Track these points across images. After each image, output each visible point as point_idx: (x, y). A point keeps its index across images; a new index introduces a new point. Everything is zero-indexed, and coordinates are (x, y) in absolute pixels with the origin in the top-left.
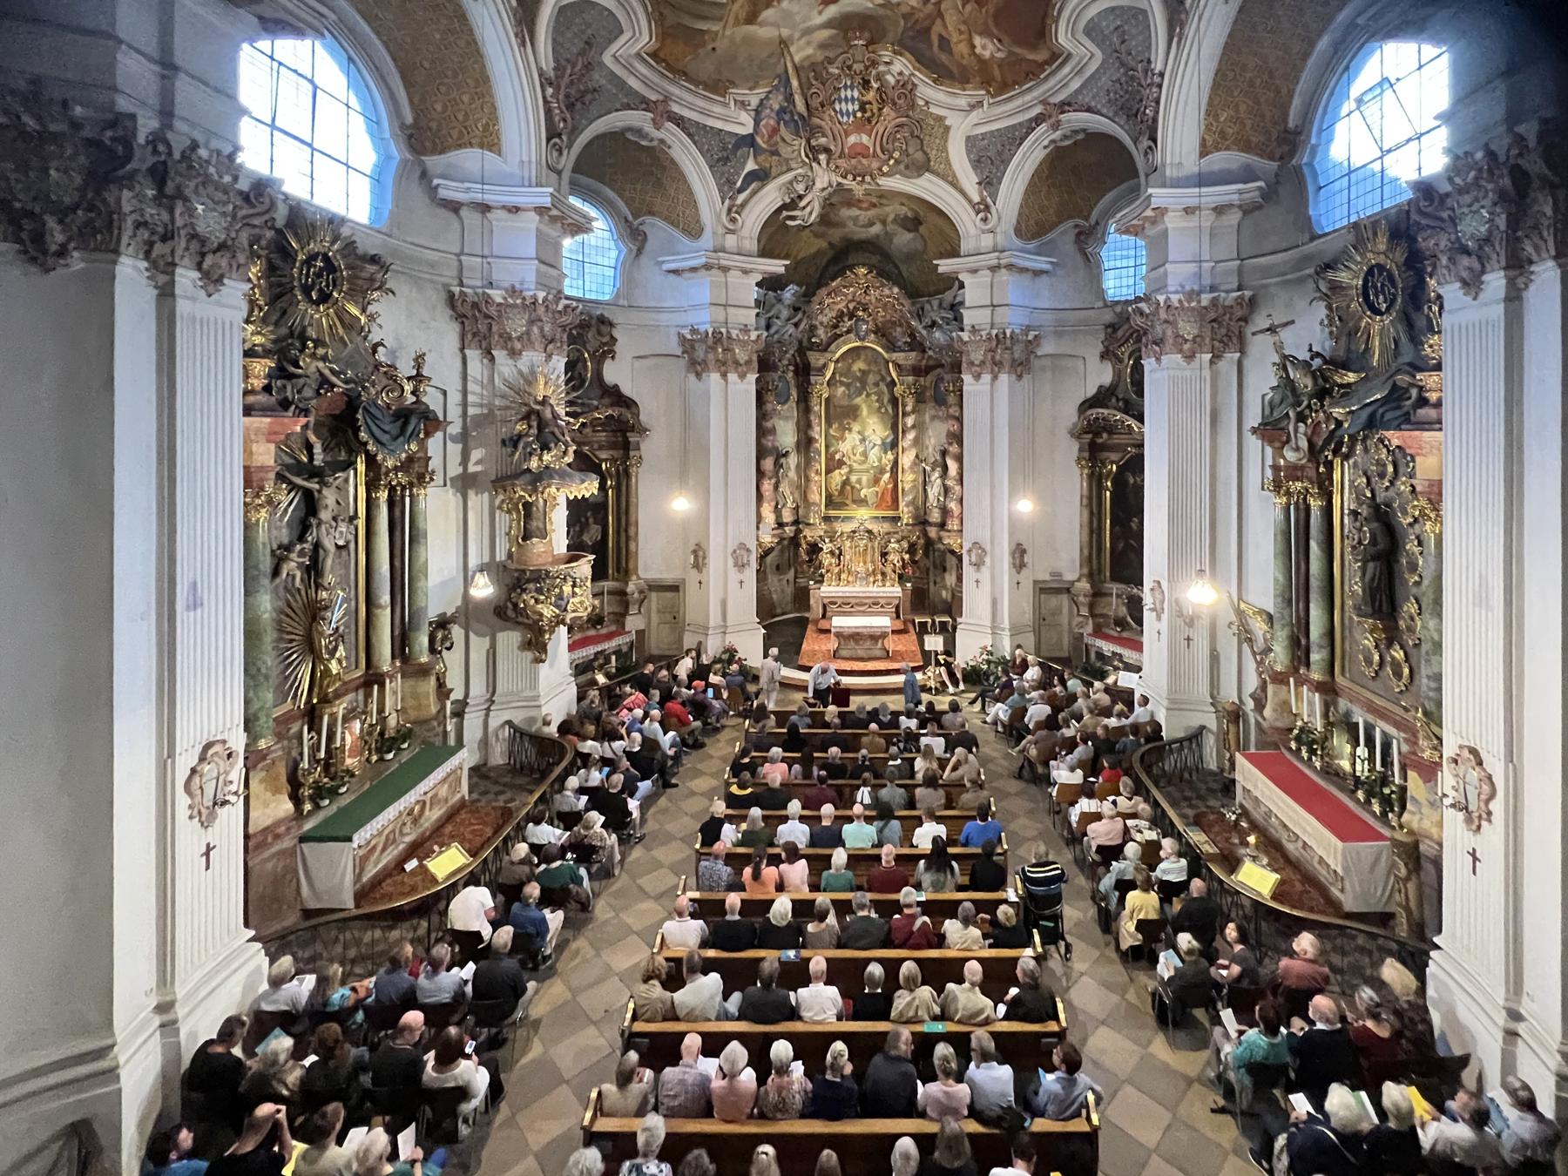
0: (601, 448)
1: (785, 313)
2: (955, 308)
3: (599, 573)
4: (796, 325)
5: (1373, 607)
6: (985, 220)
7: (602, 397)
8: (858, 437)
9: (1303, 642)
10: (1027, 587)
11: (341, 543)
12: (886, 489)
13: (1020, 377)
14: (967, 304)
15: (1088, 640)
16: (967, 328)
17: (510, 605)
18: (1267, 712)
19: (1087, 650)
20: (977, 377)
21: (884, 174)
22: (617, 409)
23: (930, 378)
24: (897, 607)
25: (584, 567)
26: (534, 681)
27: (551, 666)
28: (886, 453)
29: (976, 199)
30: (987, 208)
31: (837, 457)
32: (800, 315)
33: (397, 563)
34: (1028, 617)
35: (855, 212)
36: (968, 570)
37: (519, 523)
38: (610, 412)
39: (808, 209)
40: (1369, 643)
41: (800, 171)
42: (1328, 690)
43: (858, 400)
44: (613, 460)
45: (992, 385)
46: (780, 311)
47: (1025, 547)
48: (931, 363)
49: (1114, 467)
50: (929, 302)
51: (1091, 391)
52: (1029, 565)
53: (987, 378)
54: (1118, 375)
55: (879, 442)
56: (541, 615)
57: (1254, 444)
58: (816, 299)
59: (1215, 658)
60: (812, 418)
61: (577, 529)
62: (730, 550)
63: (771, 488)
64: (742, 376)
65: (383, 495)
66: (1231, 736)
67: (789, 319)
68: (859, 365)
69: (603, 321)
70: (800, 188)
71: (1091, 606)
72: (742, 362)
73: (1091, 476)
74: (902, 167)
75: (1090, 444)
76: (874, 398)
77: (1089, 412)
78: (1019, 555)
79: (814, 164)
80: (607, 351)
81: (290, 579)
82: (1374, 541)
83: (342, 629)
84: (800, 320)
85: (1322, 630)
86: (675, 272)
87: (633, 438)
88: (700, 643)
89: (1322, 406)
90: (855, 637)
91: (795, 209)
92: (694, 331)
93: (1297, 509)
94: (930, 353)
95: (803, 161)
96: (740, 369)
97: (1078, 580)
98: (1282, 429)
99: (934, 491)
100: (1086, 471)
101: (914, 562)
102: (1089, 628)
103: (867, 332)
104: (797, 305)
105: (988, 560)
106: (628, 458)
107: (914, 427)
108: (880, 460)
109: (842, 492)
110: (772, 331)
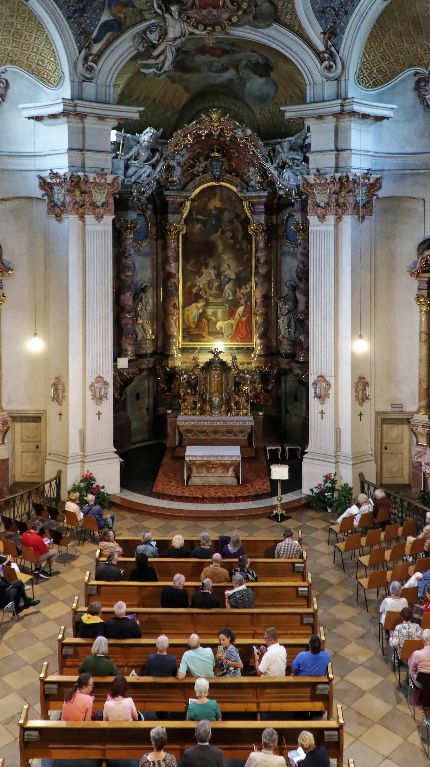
6: (329, 68)
12: (240, 321)
13: (362, 218)
16: (313, 171)
21: (233, 25)
24: (250, 435)
29: (322, 48)
30: (332, 55)
32: (157, 155)
35: (208, 58)
36: (313, 402)
39: (162, 58)
41: (153, 21)
45: (336, 225)
47: (368, 380)
50: (280, 143)
52: (372, 397)
53: (331, 219)
64: (99, 218)
67: (146, 161)
70: (153, 37)
72: (99, 204)
74: (251, 17)
79: (167, 15)
84: (158, 161)
91: (150, 57)
92: (55, 175)
94: (281, 193)
95: (156, 12)
96: (97, 210)
97: (418, 412)
100: (425, 308)
101: (267, 391)
108: (234, 293)
109: (198, 325)
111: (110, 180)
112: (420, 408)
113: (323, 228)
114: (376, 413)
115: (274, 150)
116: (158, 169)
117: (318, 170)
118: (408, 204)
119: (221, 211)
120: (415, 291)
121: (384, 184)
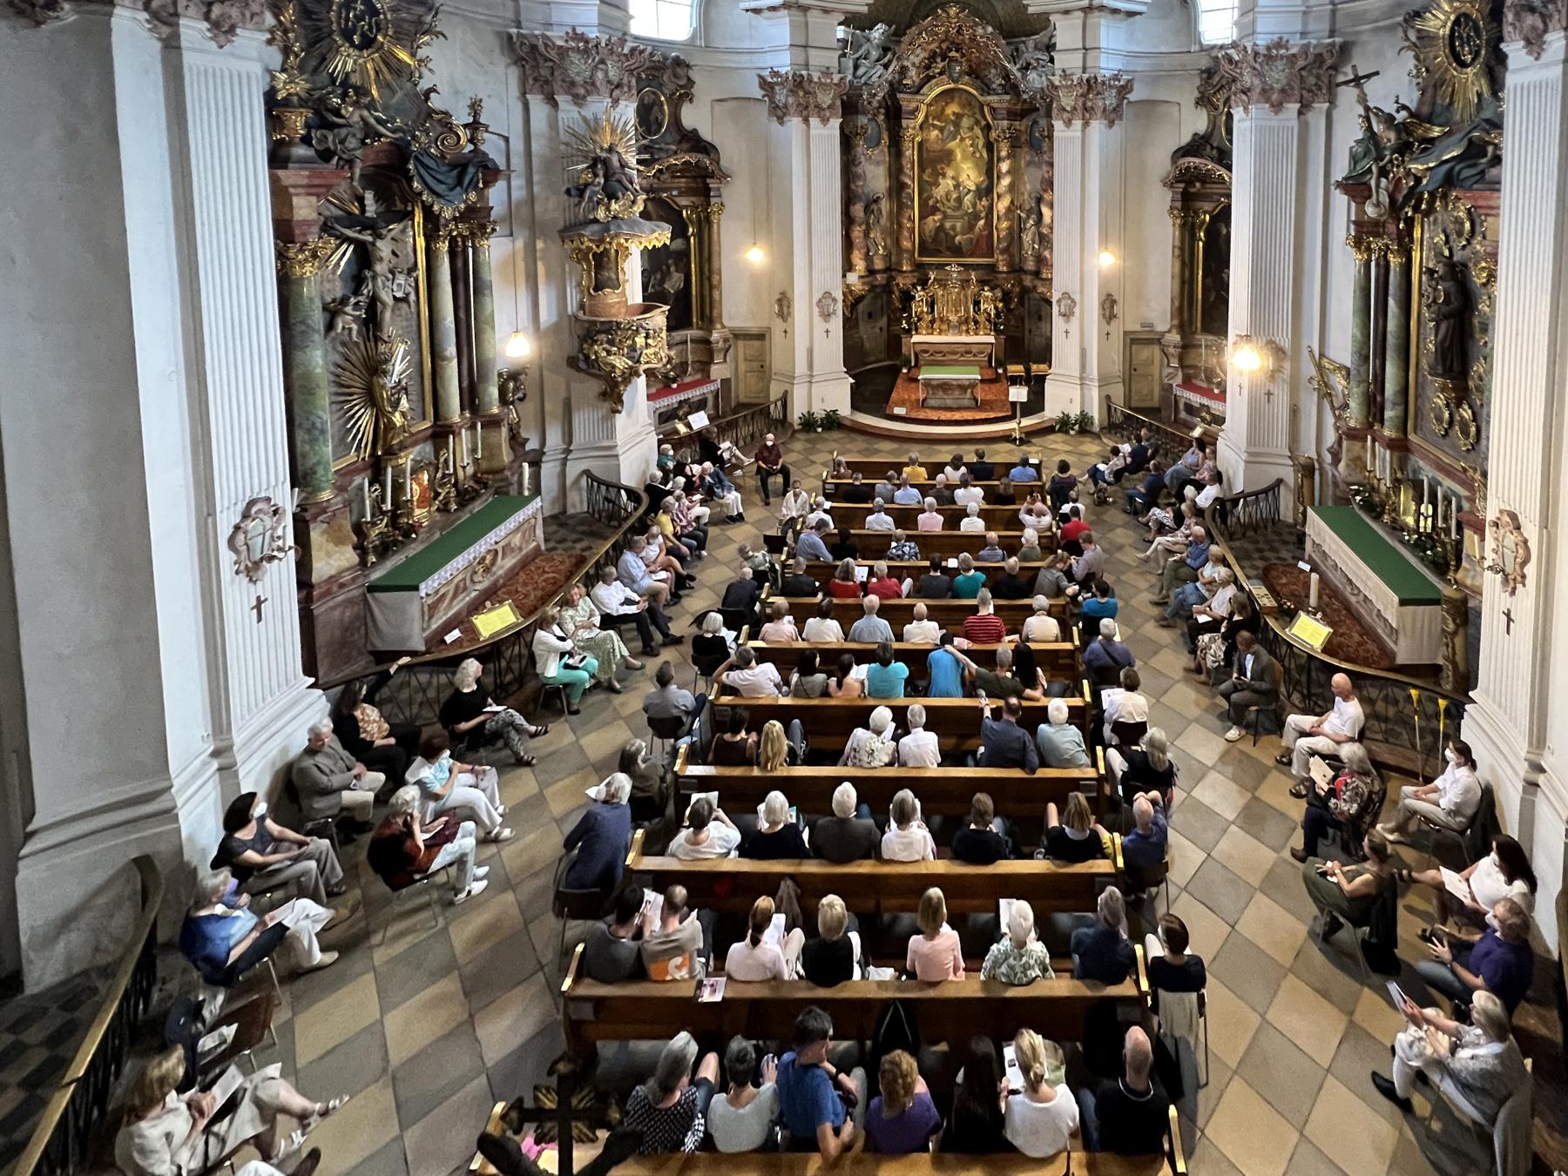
0: (680, 195)
1: (875, 54)
2: (1050, 47)
3: (677, 321)
4: (886, 66)
5: (1444, 365)
7: (680, 142)
8: (951, 183)
9: (1379, 398)
10: (1117, 341)
11: (399, 295)
13: (1111, 123)
14: (1058, 48)
15: (1179, 392)
16: (1058, 72)
17: (581, 356)
18: (1342, 466)
19: (1176, 401)
20: (1068, 123)
22: (694, 155)
23: (1027, 122)
25: (658, 318)
26: (611, 433)
27: (629, 415)
28: (980, 200)
31: (931, 203)
33: (462, 315)
34: (1117, 367)
36: (1057, 320)
37: (590, 274)
38: (687, 158)
40: (1440, 401)
42: (1400, 447)
43: (952, 145)
44: (694, 207)
45: (1083, 131)
46: (869, 52)
47: (1116, 297)
48: (1026, 106)
49: (1208, 217)
51: (1186, 139)
52: (1120, 315)
53: (1078, 123)
54: (1213, 123)
55: (973, 188)
56: (614, 367)
57: (1340, 200)
58: (906, 39)
59: (1295, 412)
60: (904, 163)
61: (659, 276)
62: (815, 300)
63: (862, 235)
64: (825, 121)
65: (444, 247)
66: (1306, 491)
67: (878, 60)
68: (952, 109)
69: (678, 62)
71: (1181, 359)
72: (825, 106)
73: (1183, 226)
75: (1182, 194)
76: (968, 142)
77: (1181, 161)
78: (1109, 306)
80: (685, 93)
81: (346, 332)
82: (1447, 301)
83: (403, 383)
84: (890, 62)
85: (1398, 388)
86: (757, 11)
87: (713, 183)
88: (786, 392)
89: (1403, 161)
90: (945, 386)
93: (1377, 265)
94: (1025, 96)
97: (1169, 331)
98: (1365, 183)
99: (1027, 238)
100: (1178, 221)
101: (1009, 310)
102: (1179, 379)
103: (961, 73)
104: (889, 45)
105: (1077, 310)
106: (709, 204)
107: (1009, 172)
108: (974, 205)
110: (861, 71)
111: (836, 81)
112: (1172, 327)
113: (1069, 134)
114: (1125, 333)
115: (1017, 50)
116: (890, 69)
117: (1064, 71)
118: (1164, 108)
119: (959, 116)
120: (1169, 204)
121: (1136, 86)
